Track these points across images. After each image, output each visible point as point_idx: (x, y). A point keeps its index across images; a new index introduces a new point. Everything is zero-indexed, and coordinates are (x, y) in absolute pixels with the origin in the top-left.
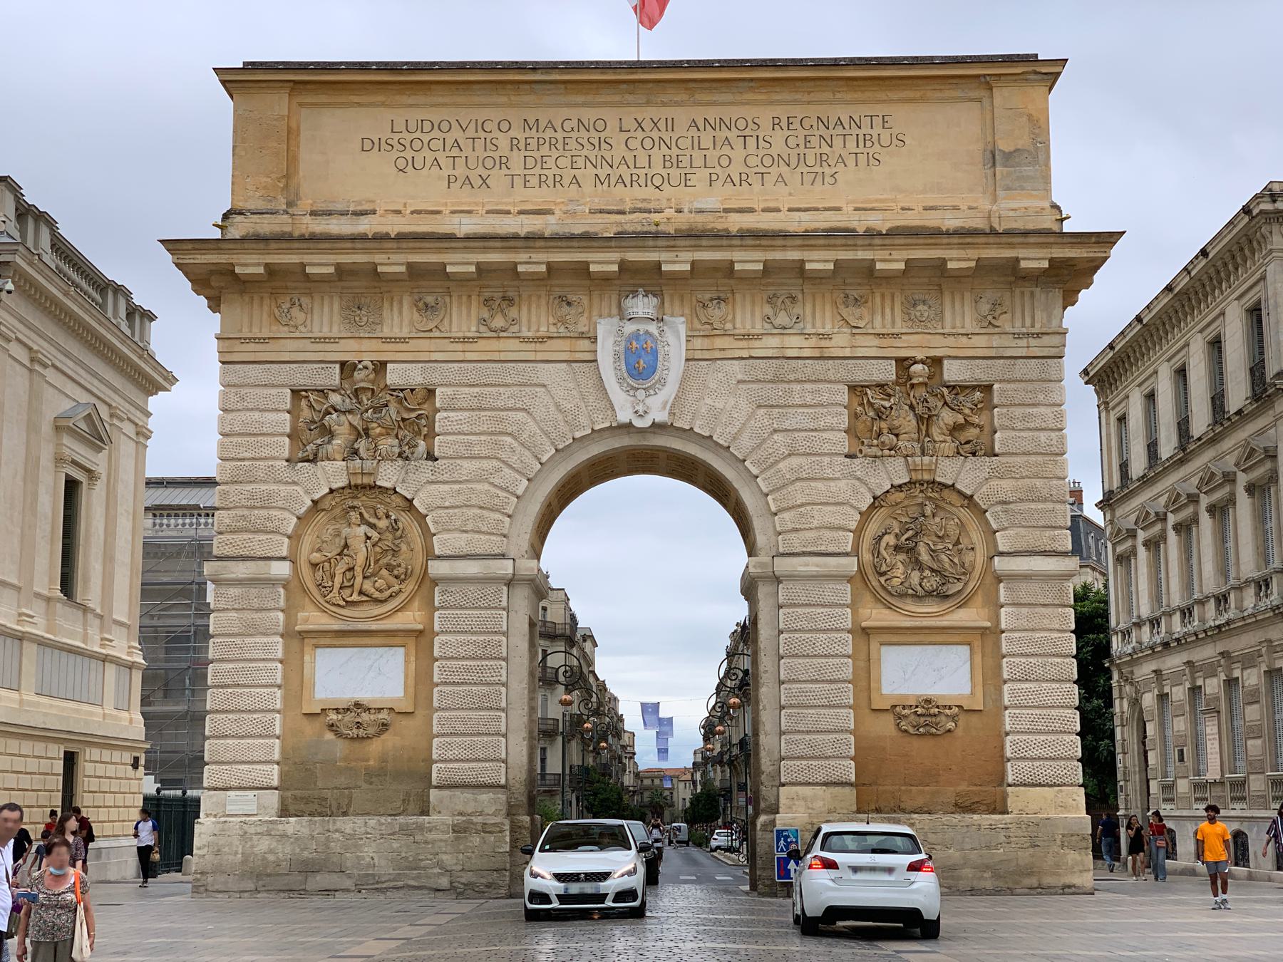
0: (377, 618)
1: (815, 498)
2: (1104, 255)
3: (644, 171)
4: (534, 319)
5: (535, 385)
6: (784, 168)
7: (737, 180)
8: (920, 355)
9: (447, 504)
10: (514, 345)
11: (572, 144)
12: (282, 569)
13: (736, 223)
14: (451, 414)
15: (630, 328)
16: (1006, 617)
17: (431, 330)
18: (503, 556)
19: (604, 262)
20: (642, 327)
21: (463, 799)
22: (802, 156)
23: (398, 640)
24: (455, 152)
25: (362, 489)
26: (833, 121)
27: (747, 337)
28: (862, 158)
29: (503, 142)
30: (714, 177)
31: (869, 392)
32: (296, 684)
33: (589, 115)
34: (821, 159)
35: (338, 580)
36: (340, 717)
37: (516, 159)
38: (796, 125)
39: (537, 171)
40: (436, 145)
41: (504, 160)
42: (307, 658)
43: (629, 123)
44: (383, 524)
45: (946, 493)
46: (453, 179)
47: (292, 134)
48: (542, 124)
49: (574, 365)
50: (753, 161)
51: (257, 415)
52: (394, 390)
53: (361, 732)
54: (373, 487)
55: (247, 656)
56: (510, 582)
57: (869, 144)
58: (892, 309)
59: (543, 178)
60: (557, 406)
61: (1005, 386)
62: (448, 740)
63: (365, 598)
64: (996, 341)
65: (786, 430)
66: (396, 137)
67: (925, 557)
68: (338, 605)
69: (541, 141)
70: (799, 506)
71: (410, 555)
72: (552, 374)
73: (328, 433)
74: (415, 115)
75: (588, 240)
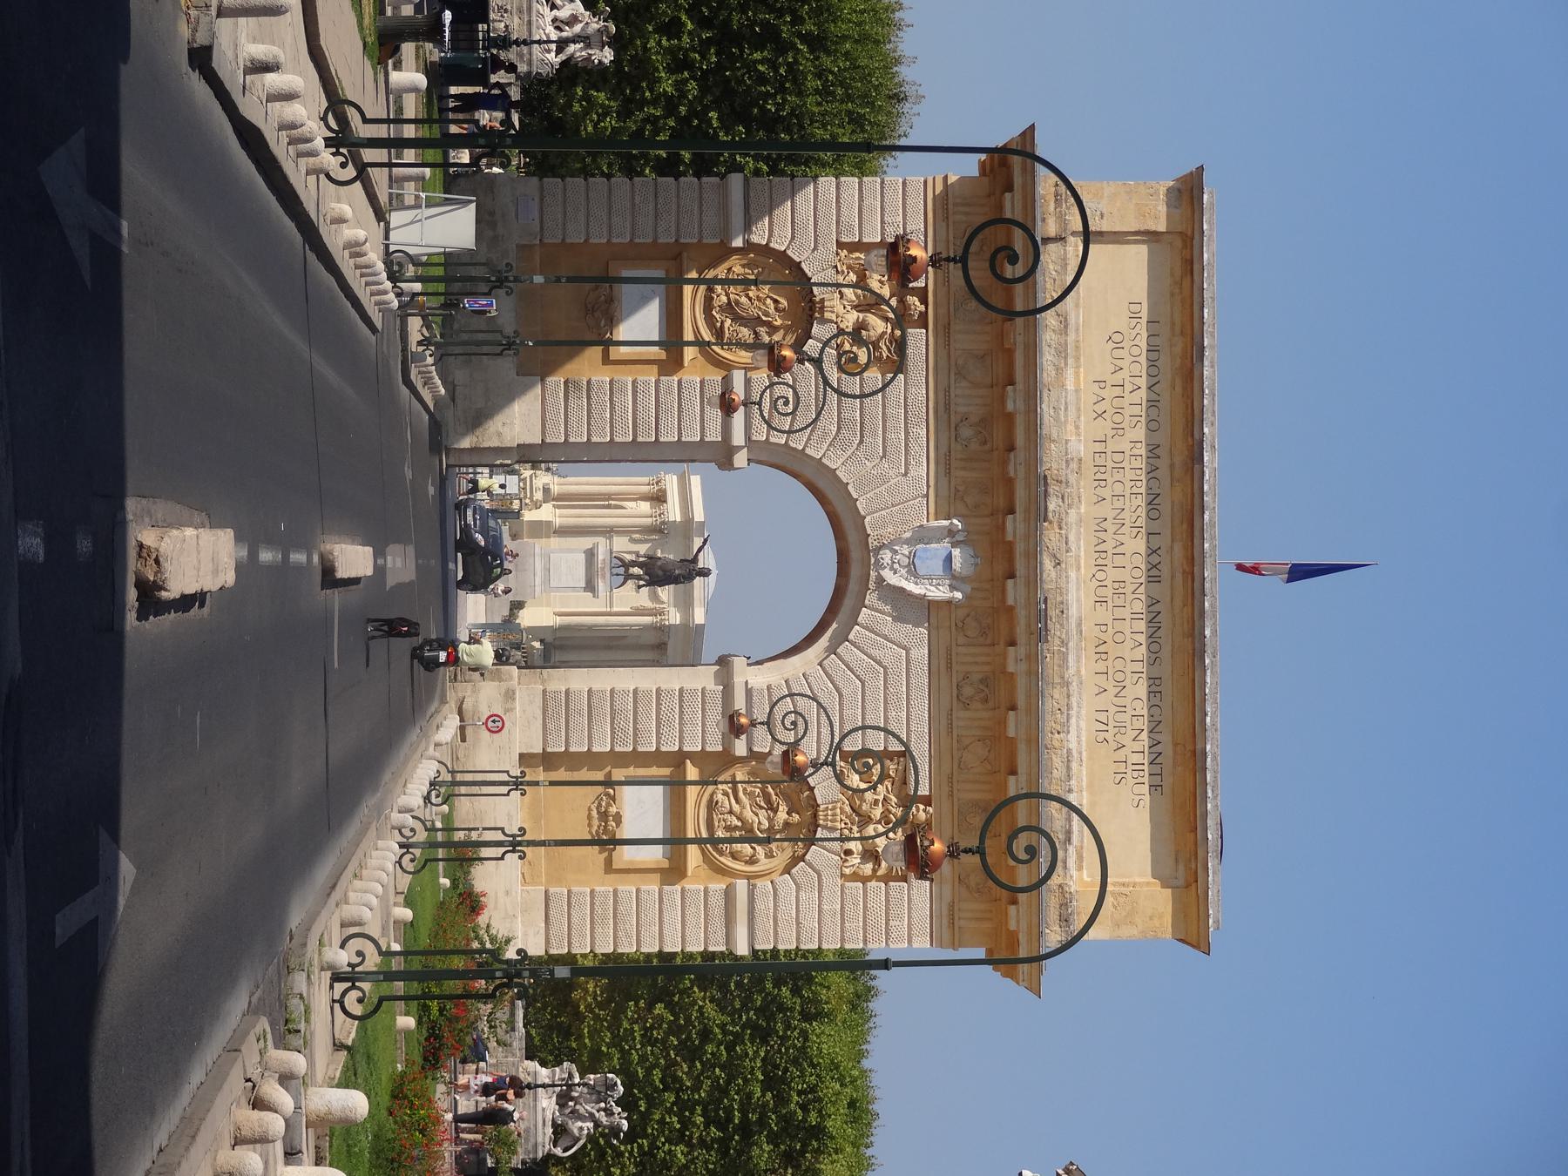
2: (1021, 978)
3: (1110, 565)
6: (1112, 691)
7: (1101, 649)
19: (1014, 526)
22: (1123, 709)
24: (1128, 387)
26: (1158, 737)
30: (1104, 628)
34: (1120, 727)
39: (1110, 464)
41: (1120, 432)
46: (1103, 385)
50: (1119, 664)
57: (1135, 774)
59: (1103, 470)
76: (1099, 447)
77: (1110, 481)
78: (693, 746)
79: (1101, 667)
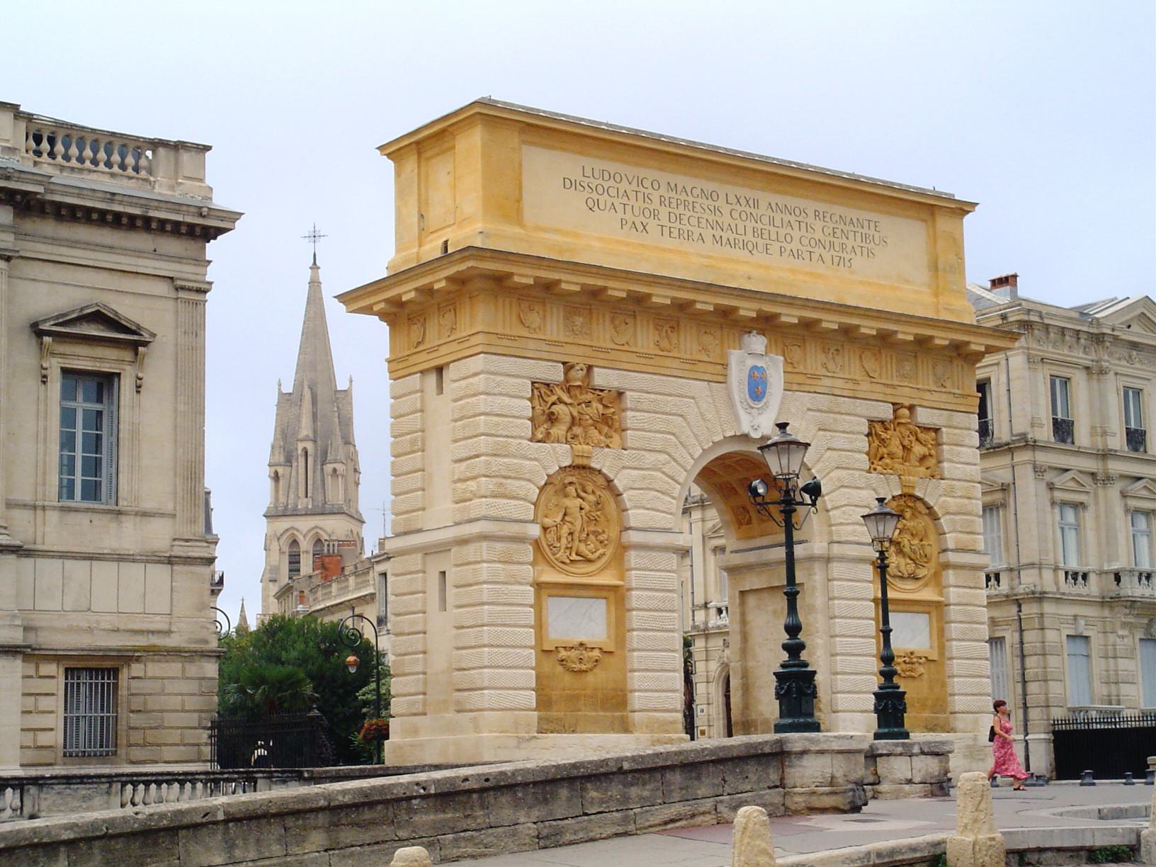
0: (588, 574)
1: (851, 501)
3: (743, 237)
4: (688, 345)
5: (689, 397)
6: (822, 251)
8: (907, 402)
9: (636, 486)
10: (676, 364)
11: (698, 208)
12: (535, 531)
14: (638, 414)
15: (751, 362)
16: (953, 594)
17: (623, 345)
20: (760, 364)
23: (604, 594)
24: (625, 200)
25: (581, 468)
26: (848, 220)
27: (816, 377)
28: (865, 250)
29: (655, 197)
31: (876, 425)
33: (709, 186)
35: (564, 541)
36: (569, 653)
37: (664, 212)
38: (827, 219)
40: (613, 192)
41: (656, 213)
42: (544, 604)
43: (732, 199)
44: (591, 498)
45: (919, 505)
48: (679, 189)
49: (711, 383)
50: (805, 241)
51: (507, 400)
52: (596, 390)
53: (584, 667)
54: (590, 468)
55: (511, 601)
57: (868, 241)
58: (891, 367)
59: (681, 232)
60: (702, 415)
61: (949, 430)
62: (644, 674)
63: (581, 558)
64: (944, 397)
65: (835, 449)
66: (587, 180)
67: (907, 550)
68: (563, 563)
69: (679, 202)
70: (842, 506)
72: (698, 388)
73: (552, 418)
74: (599, 165)
76: (666, 231)
77: (690, 228)
79: (806, 255)
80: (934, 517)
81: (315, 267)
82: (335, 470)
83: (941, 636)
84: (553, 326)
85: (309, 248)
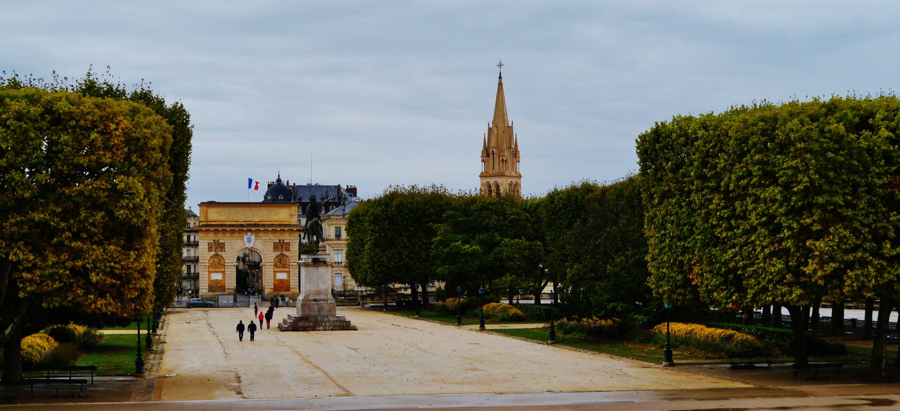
12: (208, 264)
13: (260, 223)
15: (248, 236)
16: (291, 270)
18: (233, 263)
21: (229, 290)
25: (216, 255)
27: (262, 237)
32: (209, 277)
47: (207, 212)
56: (234, 266)
71: (222, 262)
73: (212, 248)
74: (221, 209)
75: (242, 226)
78: (273, 270)
80: (288, 258)
81: (500, 78)
82: (503, 159)
83: (289, 276)
84: (212, 235)
85: (498, 69)
